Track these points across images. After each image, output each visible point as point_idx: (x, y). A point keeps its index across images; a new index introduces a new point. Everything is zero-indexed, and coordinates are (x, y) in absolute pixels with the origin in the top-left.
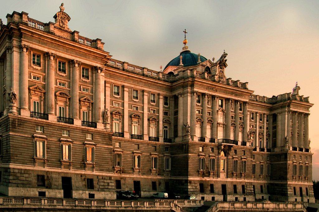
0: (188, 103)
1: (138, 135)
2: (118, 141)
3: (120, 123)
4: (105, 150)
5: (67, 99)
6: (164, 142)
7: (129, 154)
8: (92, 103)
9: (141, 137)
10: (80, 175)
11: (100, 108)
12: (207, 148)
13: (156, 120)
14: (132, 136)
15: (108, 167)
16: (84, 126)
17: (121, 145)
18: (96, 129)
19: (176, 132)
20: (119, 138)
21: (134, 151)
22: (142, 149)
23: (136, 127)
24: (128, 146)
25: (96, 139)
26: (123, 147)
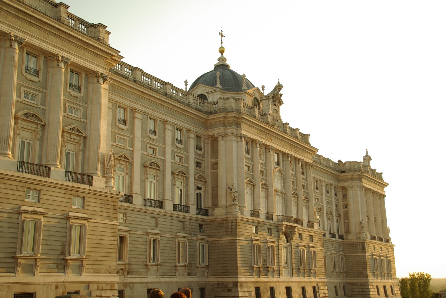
0: (234, 152)
1: (156, 200)
2: (123, 211)
3: (127, 177)
4: (105, 230)
5: (39, 127)
6: (198, 214)
7: (141, 236)
8: (85, 138)
9: (160, 204)
10: (54, 286)
11: (99, 148)
12: (263, 228)
13: (184, 174)
14: (147, 202)
15: (109, 263)
16: (70, 181)
17: (128, 218)
18: (91, 188)
19: (215, 197)
20: (124, 204)
21: (150, 231)
22: (162, 226)
23: (152, 184)
24: (140, 220)
25: (91, 208)
26: (131, 222)
